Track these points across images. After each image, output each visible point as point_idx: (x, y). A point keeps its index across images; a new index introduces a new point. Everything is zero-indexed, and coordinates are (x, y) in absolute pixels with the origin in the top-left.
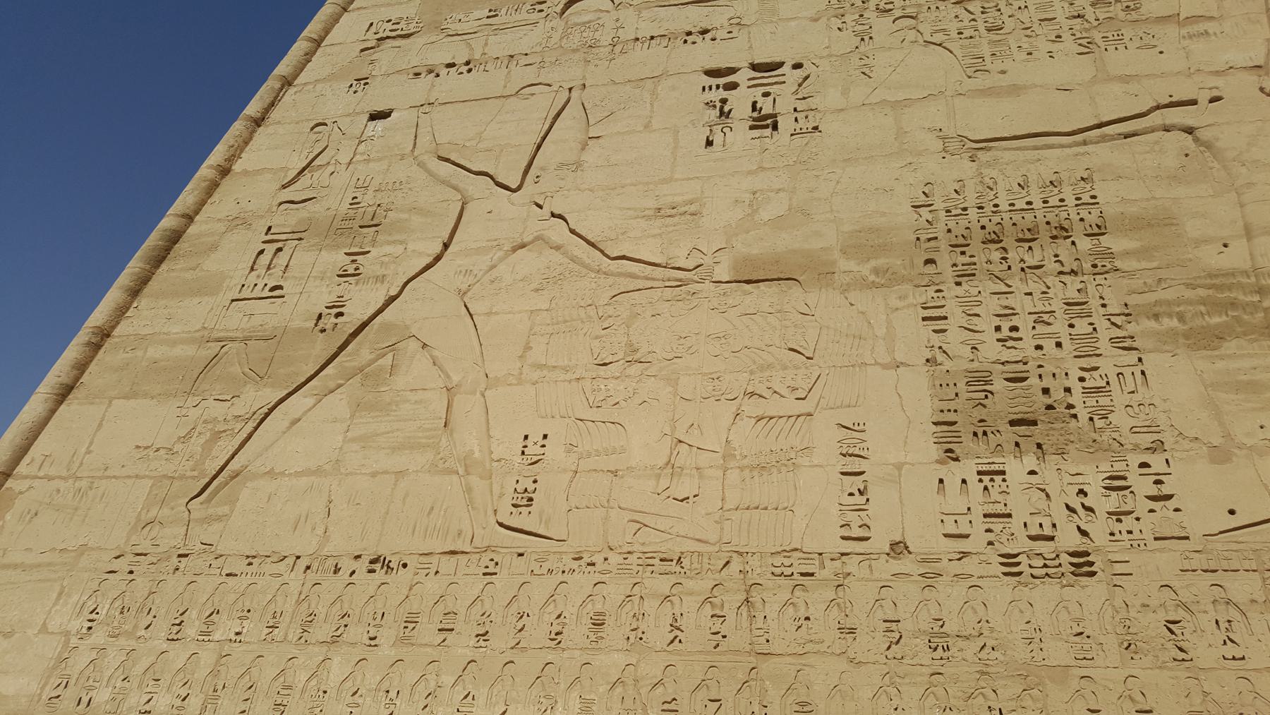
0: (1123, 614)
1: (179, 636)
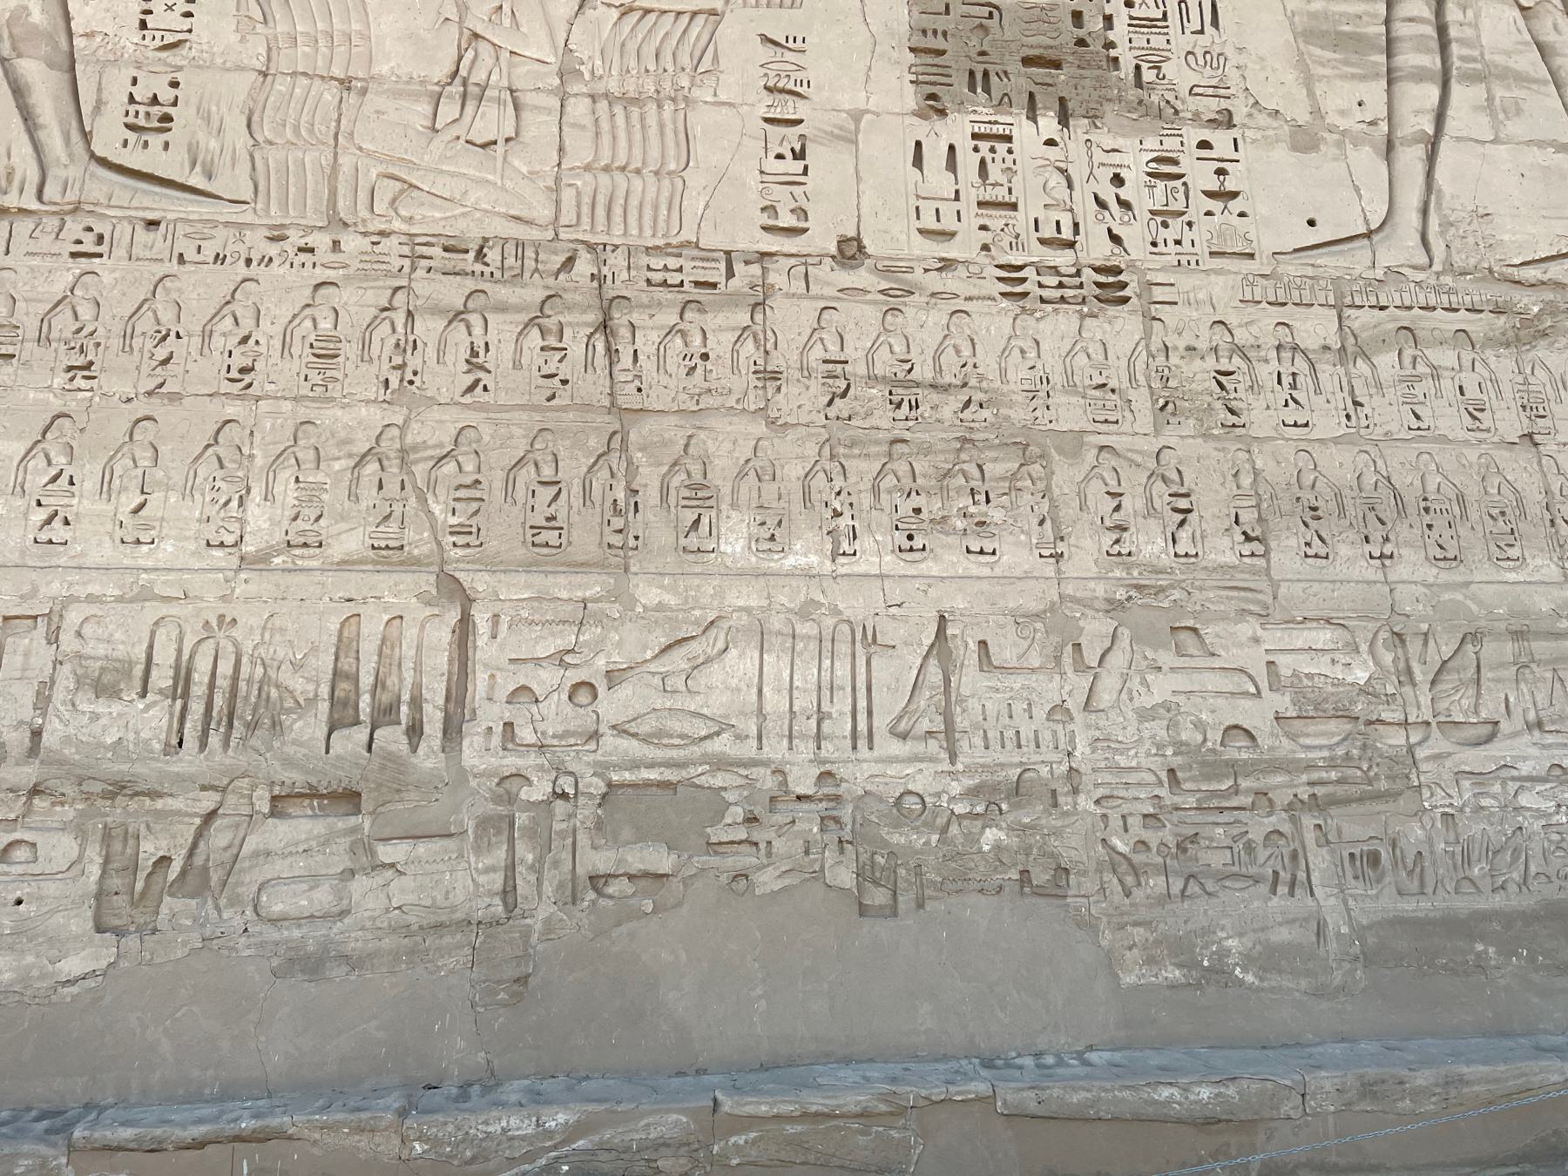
0: (1161, 359)
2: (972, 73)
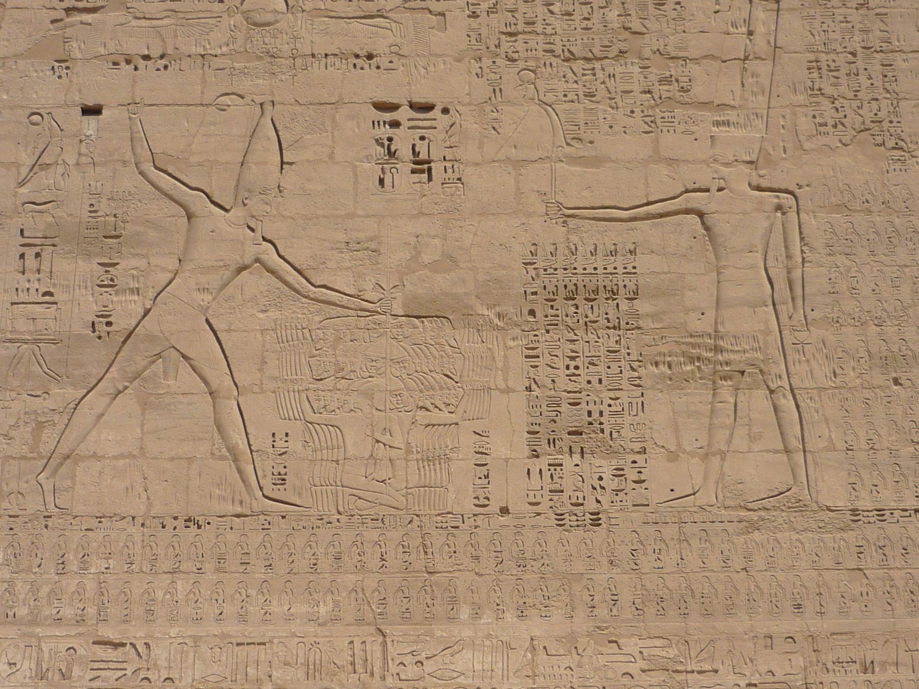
1: (65, 571)
2: (549, 440)
